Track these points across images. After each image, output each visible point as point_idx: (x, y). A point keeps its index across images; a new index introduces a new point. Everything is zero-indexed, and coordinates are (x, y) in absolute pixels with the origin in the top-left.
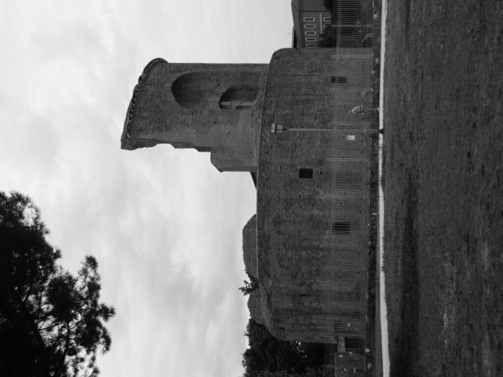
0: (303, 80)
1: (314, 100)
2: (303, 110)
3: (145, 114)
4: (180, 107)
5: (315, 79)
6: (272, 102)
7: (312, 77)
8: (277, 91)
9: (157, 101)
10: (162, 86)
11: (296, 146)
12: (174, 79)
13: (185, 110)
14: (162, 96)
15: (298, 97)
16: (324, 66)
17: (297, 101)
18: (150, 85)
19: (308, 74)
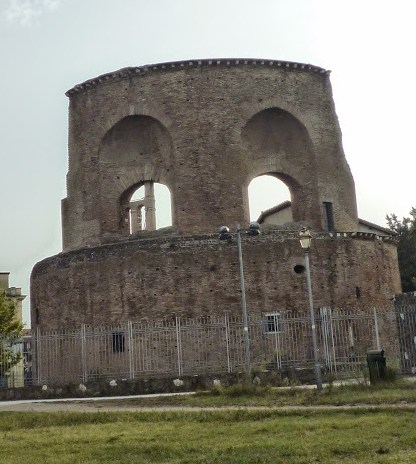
0: (113, 294)
1: (85, 314)
2: (73, 302)
3: (89, 102)
4: (98, 140)
5: (116, 309)
6: (83, 260)
7: (121, 305)
8: (95, 263)
9: (106, 108)
10: (130, 102)
11: (48, 300)
12: (146, 112)
13: (96, 149)
14: (114, 111)
15: (88, 291)
16: (146, 318)
17: (84, 292)
18: (130, 86)
19: (125, 299)
